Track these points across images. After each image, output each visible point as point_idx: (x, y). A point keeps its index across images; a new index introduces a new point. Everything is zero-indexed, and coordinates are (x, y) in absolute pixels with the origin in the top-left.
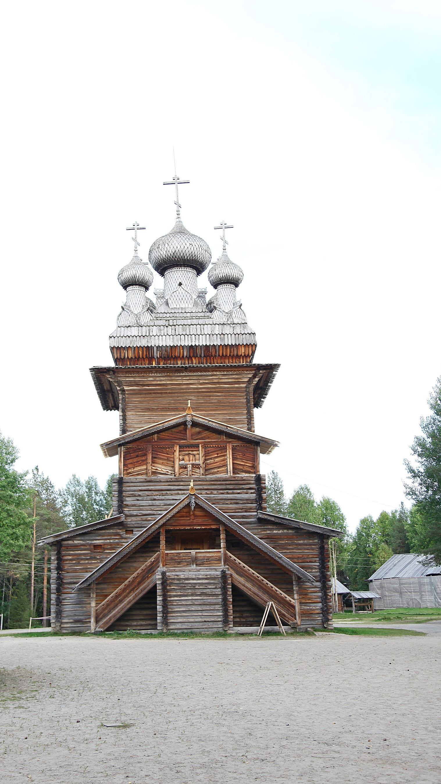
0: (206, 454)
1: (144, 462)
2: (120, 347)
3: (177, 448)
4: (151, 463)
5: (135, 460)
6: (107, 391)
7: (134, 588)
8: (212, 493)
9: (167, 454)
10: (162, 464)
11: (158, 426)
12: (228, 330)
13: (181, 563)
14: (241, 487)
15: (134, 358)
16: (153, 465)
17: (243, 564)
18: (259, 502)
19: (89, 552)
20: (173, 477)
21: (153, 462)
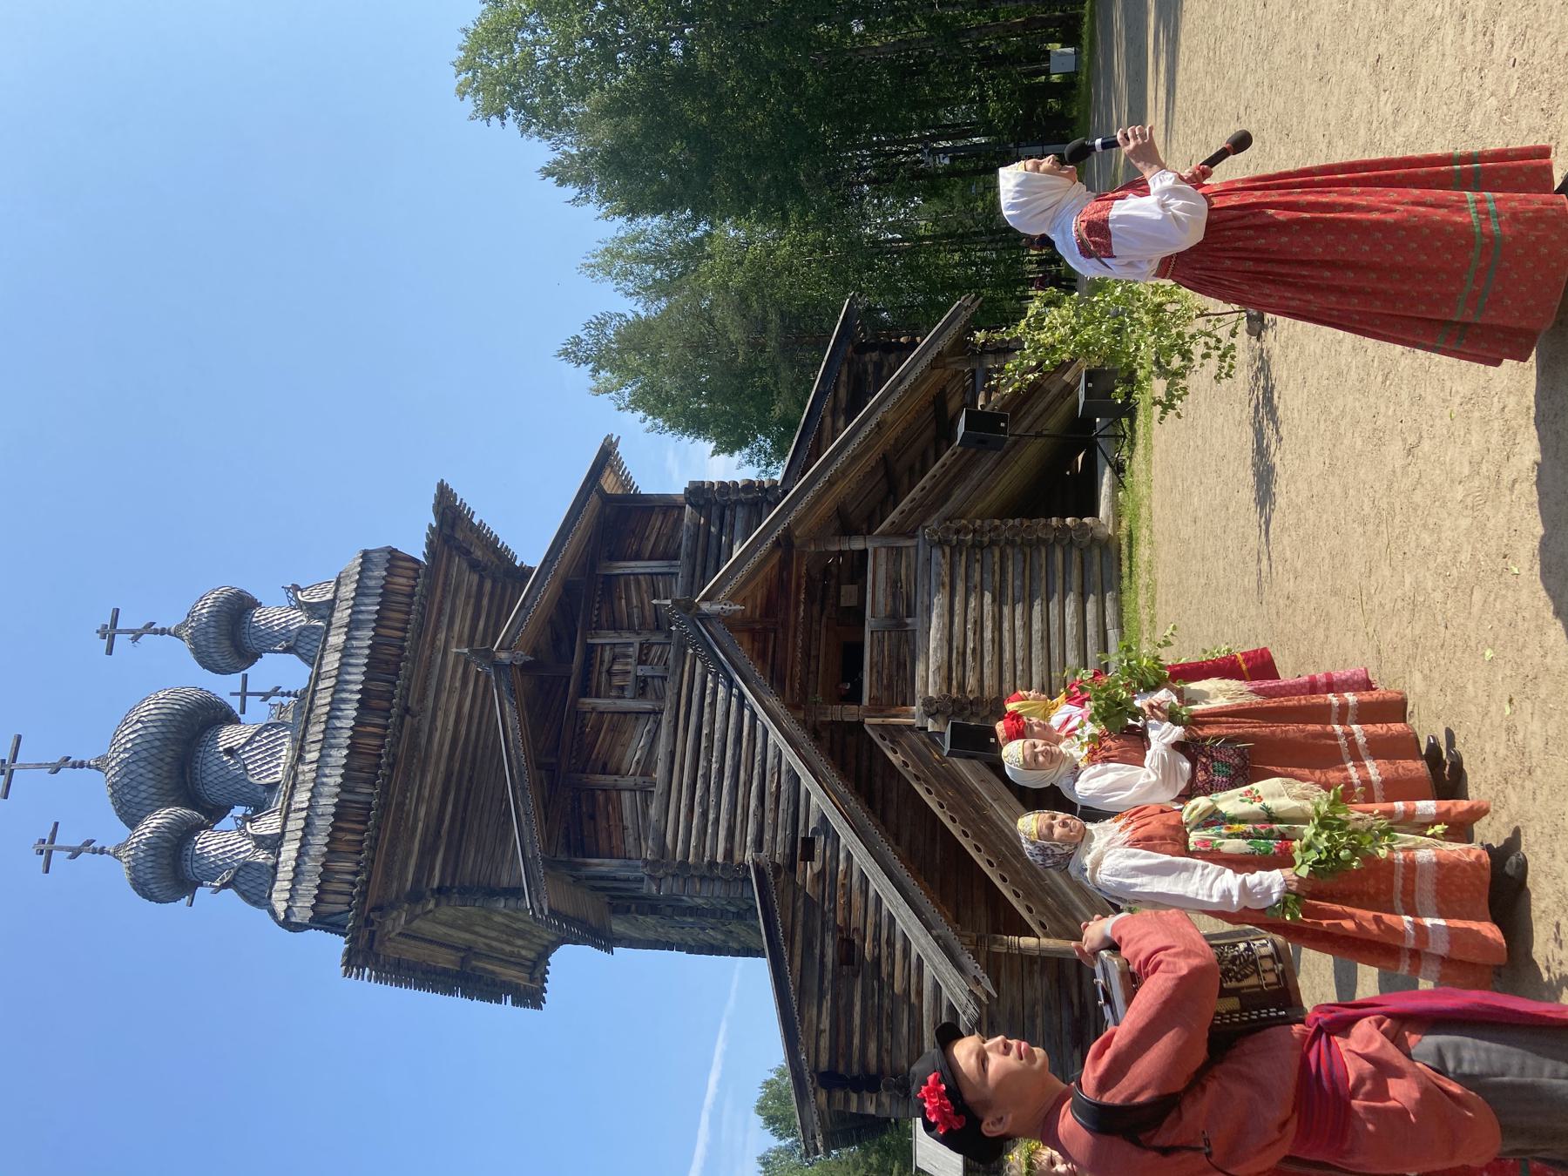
0: (615, 626)
2: (317, 892)
3: (588, 702)
4: (616, 777)
5: (602, 824)
6: (461, 967)
9: (599, 731)
10: (625, 746)
13: (902, 661)
16: (623, 772)
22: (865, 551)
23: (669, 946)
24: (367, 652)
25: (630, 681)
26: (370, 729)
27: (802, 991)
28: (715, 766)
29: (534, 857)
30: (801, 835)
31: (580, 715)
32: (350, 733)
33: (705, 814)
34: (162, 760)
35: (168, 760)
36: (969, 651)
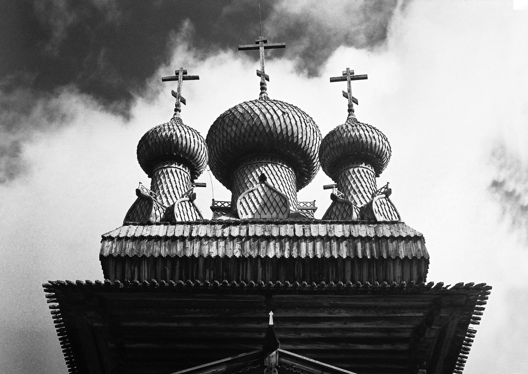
12: (362, 231)
24: (327, 255)
26: (260, 270)
32: (254, 256)
34: (255, 135)
35: (257, 139)
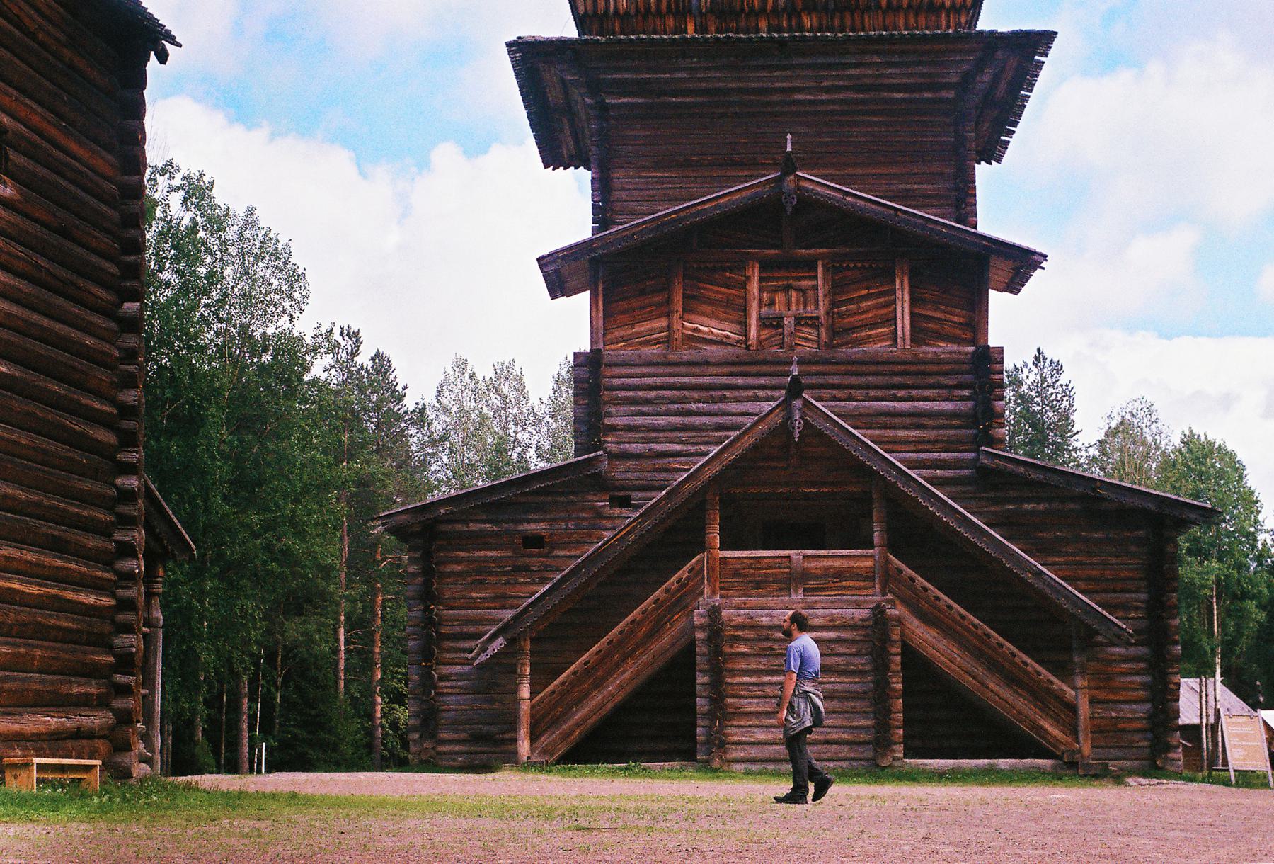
0: (836, 290)
1: (665, 310)
3: (755, 273)
7: (634, 651)
8: (850, 399)
9: (728, 287)
10: (713, 316)
11: (700, 208)
13: (762, 586)
14: (932, 380)
15: (632, 12)
16: (686, 316)
17: (933, 590)
18: (984, 425)
19: (509, 554)
20: (741, 351)
21: (684, 310)
22: (872, 547)
23: (591, 334)
25: (779, 309)
27: (498, 505)
28: (694, 406)
29: (594, 250)
30: (633, 494)
31: (741, 266)
33: (648, 402)
36: (769, 644)
